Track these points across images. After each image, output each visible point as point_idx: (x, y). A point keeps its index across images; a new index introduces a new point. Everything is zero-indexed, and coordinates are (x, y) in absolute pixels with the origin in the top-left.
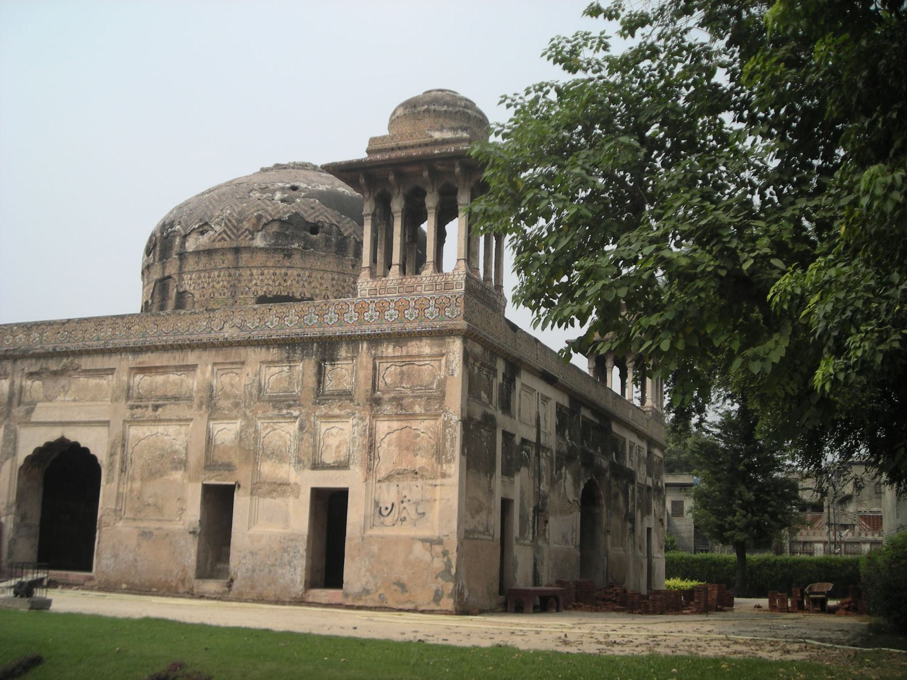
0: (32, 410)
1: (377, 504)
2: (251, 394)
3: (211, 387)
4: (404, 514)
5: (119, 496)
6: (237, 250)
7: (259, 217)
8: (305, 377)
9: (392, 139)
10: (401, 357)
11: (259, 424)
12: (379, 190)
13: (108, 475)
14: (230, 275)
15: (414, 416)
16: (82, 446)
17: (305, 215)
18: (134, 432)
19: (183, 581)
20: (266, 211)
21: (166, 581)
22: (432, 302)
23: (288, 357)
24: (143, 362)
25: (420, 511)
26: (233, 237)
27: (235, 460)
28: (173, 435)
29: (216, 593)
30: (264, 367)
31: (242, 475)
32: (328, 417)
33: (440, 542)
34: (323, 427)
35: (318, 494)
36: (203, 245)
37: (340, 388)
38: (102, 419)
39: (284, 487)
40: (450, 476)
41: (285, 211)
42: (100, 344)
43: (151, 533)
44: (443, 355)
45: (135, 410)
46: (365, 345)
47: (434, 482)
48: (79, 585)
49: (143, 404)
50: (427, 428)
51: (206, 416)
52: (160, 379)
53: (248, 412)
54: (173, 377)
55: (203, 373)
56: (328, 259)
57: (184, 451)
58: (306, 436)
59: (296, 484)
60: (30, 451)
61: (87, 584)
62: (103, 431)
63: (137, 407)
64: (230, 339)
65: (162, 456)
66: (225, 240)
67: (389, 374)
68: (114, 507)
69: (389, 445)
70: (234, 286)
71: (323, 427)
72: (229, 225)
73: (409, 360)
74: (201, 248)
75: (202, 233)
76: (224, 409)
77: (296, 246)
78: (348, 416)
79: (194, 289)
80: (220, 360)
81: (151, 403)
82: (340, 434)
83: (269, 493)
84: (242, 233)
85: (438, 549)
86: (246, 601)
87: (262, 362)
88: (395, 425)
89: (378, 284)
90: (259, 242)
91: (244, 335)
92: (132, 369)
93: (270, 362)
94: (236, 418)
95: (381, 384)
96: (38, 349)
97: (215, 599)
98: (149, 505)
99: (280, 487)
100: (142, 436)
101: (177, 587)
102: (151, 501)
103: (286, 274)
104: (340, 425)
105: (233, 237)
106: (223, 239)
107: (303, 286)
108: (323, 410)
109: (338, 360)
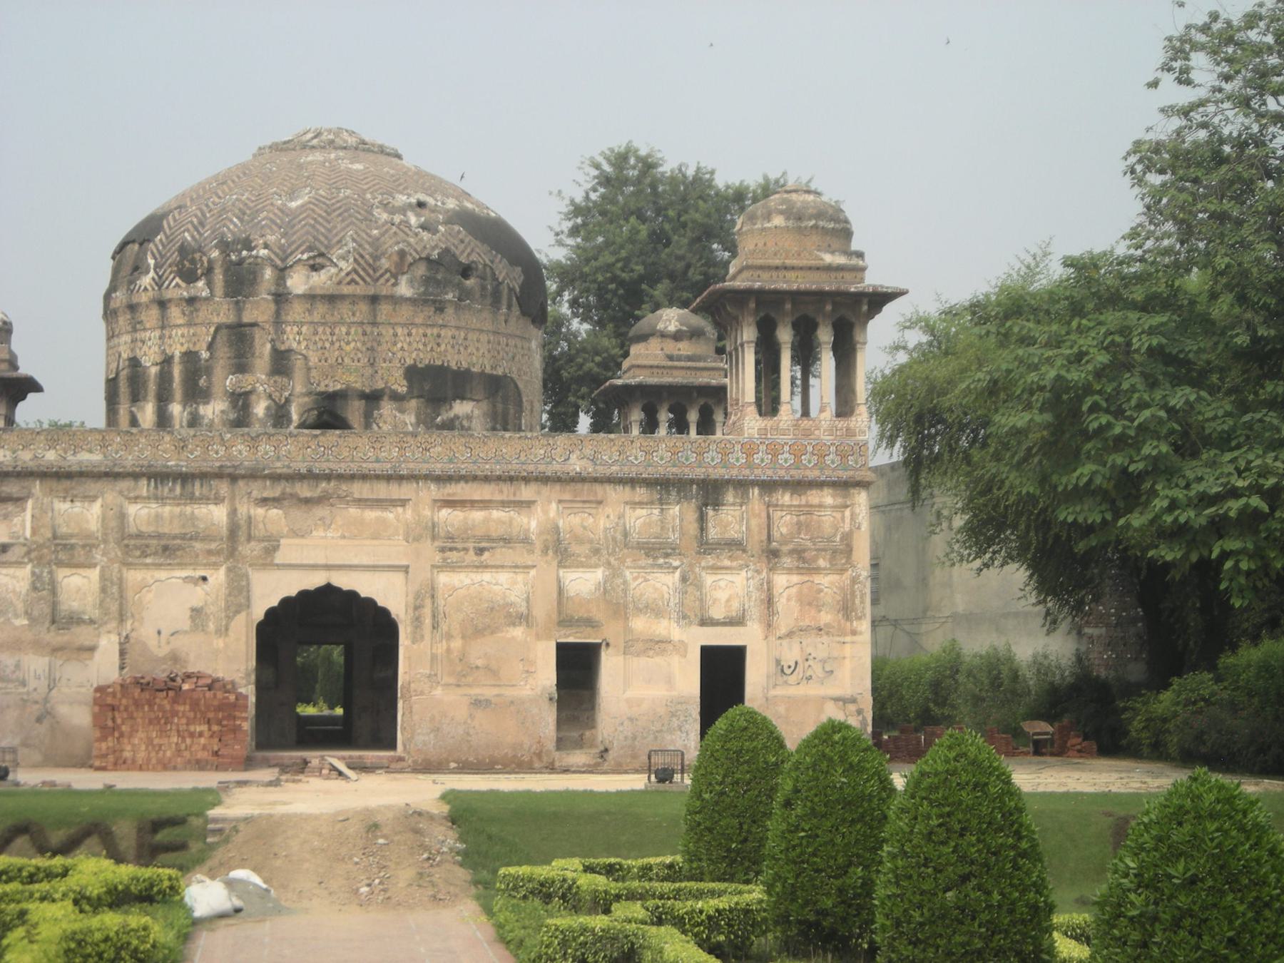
0: (276, 548)
1: (778, 662)
2: (614, 539)
3: (556, 529)
4: (808, 674)
5: (434, 658)
6: (374, 300)
7: (402, 254)
8: (685, 523)
9: (775, 254)
10: (799, 506)
11: (627, 573)
12: (762, 314)
13: (414, 633)
14: (364, 334)
15: (817, 570)
16: (363, 595)
17: (457, 253)
18: (444, 579)
19: (539, 755)
20: (409, 244)
21: (515, 756)
22: (833, 449)
23: (660, 499)
24: (454, 494)
25: (828, 669)
26: (368, 279)
27: (598, 614)
28: (504, 584)
29: (584, 765)
30: (627, 507)
31: (608, 631)
32: (715, 569)
33: (853, 701)
34: (709, 579)
35: (709, 655)
36: (322, 288)
37: (727, 536)
38: (397, 563)
39: (663, 646)
40: (861, 633)
41: (430, 243)
42: (387, 468)
43: (488, 702)
44: (847, 507)
45: (448, 554)
46: (756, 491)
47: (842, 639)
48: (386, 768)
49: (459, 546)
50: (832, 583)
51: (555, 563)
52: (477, 515)
53: (612, 559)
54: (496, 514)
55: (546, 512)
56: (486, 314)
57: (524, 604)
58: (690, 589)
59: (681, 642)
60: (275, 603)
61: (393, 766)
62: (398, 578)
63: (451, 549)
64: (584, 474)
65: (492, 609)
66: (357, 283)
67: (784, 524)
68: (428, 672)
69: (789, 600)
70: (372, 349)
71: (709, 579)
72: (362, 262)
73: (809, 509)
74: (319, 292)
75: (314, 268)
76: (579, 555)
77: (450, 296)
78: (741, 568)
79: (307, 347)
80: (567, 497)
81: (471, 545)
82: (729, 587)
83: (643, 652)
84: (382, 276)
85: (852, 708)
86: (626, 772)
87: (626, 503)
88: (795, 578)
89: (768, 423)
90: (404, 289)
91: (601, 471)
92: (435, 501)
93: (636, 503)
94: (596, 566)
95: (776, 534)
96: (279, 467)
97: (584, 772)
98: (477, 667)
99: (658, 645)
100: (457, 584)
101: (531, 762)
102: (480, 663)
103: (439, 336)
104: (729, 577)
105: (368, 279)
106: (353, 281)
107: (459, 352)
108: (710, 560)
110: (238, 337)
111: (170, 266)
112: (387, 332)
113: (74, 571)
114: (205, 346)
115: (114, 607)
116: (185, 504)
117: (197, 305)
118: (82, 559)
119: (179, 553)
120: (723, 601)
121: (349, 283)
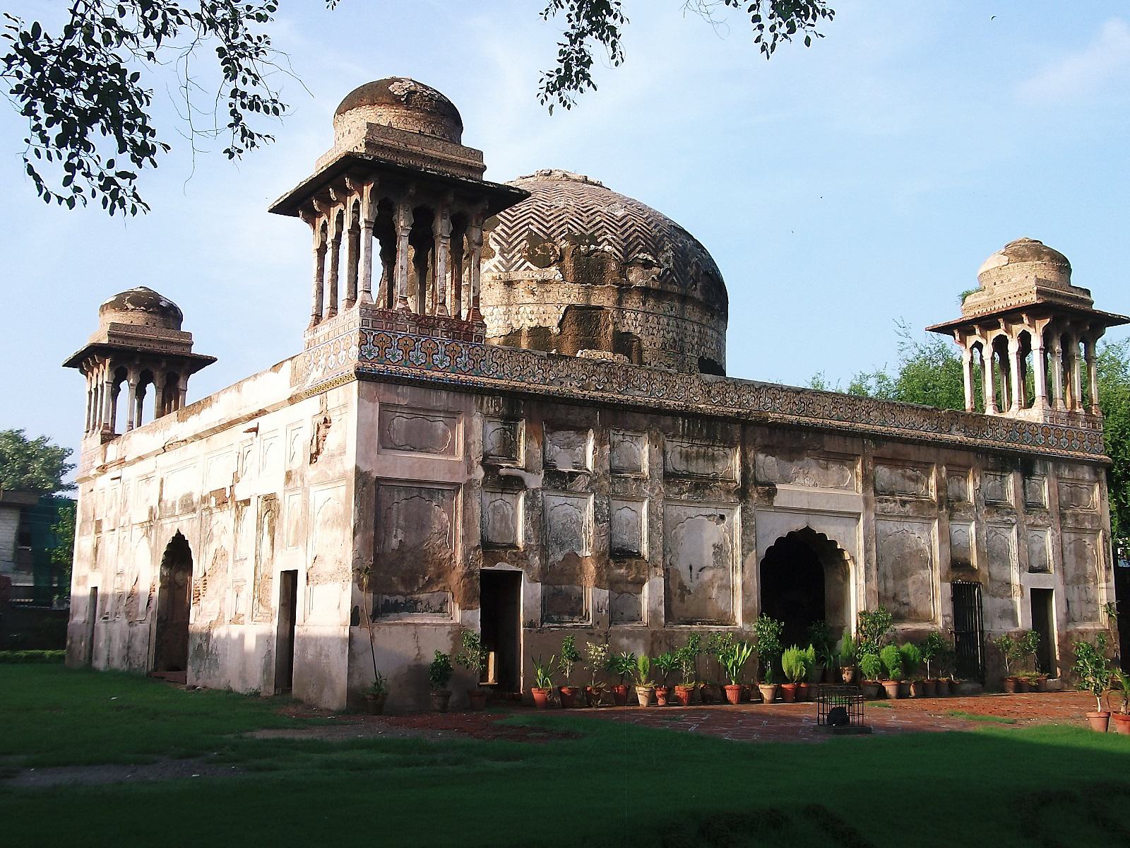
53: (979, 516)
70: (681, 340)
88: (1072, 536)
90: (697, 295)
104: (1040, 534)
109: (1035, 475)
110: (583, 319)
111: (519, 252)
112: (690, 327)
113: (625, 504)
114: (556, 323)
115: (659, 542)
116: (708, 446)
117: (548, 287)
118: (634, 493)
119: (707, 492)
120: (1037, 552)
121: (670, 283)
